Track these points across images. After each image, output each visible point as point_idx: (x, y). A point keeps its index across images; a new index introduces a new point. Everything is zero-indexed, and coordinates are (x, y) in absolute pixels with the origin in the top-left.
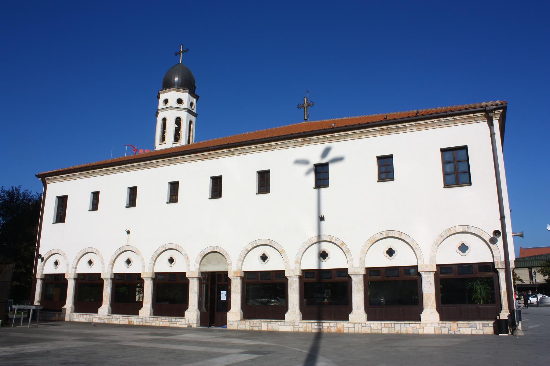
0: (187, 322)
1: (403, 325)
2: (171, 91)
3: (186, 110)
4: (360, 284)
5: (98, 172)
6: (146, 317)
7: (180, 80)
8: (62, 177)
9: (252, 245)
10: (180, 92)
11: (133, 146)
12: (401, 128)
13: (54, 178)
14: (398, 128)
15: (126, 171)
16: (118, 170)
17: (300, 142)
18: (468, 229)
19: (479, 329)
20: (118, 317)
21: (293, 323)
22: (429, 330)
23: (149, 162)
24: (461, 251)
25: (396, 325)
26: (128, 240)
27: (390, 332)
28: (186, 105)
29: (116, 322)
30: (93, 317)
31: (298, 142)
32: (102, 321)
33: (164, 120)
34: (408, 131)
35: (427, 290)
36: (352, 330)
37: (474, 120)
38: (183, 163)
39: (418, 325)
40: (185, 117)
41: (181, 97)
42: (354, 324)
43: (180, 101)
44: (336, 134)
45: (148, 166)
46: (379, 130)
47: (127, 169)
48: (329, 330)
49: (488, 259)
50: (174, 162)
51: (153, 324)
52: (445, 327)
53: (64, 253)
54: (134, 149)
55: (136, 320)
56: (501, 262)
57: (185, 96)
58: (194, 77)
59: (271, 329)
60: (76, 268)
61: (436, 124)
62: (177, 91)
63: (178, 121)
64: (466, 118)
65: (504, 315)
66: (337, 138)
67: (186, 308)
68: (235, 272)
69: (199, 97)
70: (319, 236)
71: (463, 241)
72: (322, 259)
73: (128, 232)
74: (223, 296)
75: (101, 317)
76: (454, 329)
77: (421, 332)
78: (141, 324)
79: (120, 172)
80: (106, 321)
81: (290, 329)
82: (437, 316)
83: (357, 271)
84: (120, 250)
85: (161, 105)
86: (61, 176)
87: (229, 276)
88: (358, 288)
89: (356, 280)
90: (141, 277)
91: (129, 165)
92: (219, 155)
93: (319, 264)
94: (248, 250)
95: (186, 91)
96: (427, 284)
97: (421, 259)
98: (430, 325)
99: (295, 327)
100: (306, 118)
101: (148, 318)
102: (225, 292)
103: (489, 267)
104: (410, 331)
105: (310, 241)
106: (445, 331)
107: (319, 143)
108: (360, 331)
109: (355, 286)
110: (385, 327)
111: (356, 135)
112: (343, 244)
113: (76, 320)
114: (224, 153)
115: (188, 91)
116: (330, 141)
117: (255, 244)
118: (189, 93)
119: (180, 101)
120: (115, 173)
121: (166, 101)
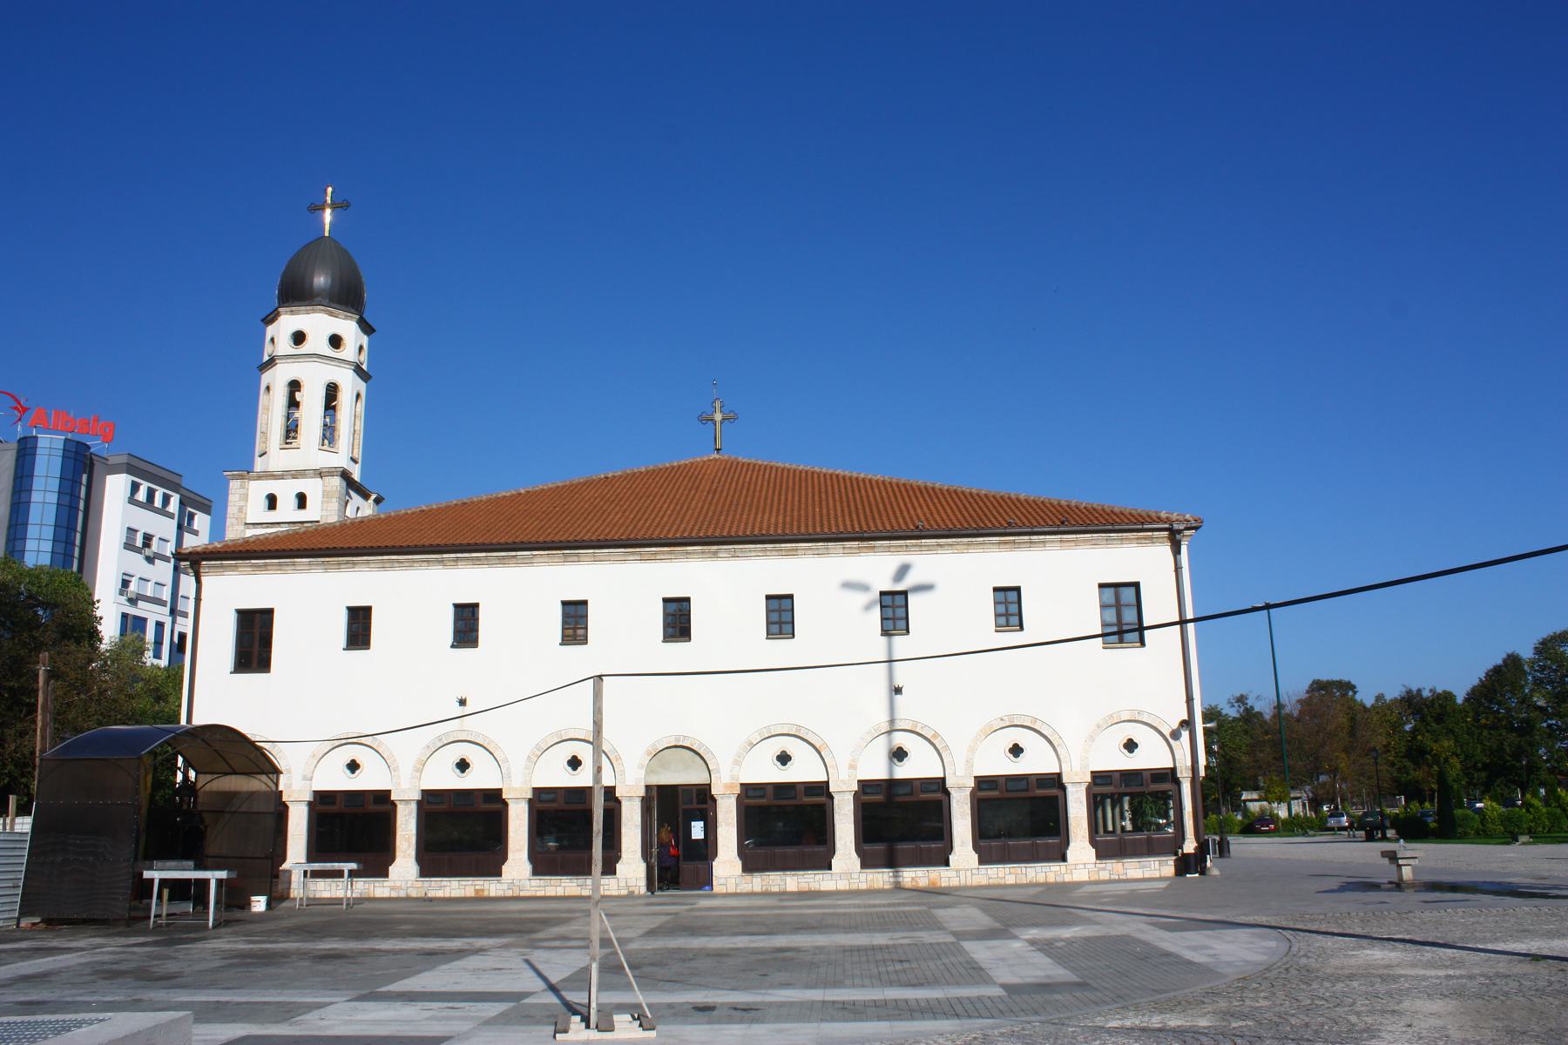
0: (622, 884)
1: (1039, 869)
2: (314, 311)
4: (966, 804)
5: (368, 562)
6: (521, 880)
7: (329, 281)
8: (253, 566)
9: (760, 734)
10: (337, 317)
11: (13, 397)
12: (1035, 543)
13: (230, 566)
14: (1031, 543)
19: (1155, 870)
20: (444, 883)
21: (848, 875)
22: (1080, 875)
23: (514, 553)
25: (1028, 869)
27: (1018, 882)
28: (349, 352)
29: (440, 894)
32: (402, 894)
36: (955, 882)
37: (1152, 540)
39: (1063, 868)
40: (349, 384)
41: (339, 332)
42: (958, 871)
43: (336, 341)
44: (923, 541)
45: (506, 561)
46: (1000, 543)
48: (914, 884)
49: (1167, 763)
50: (576, 559)
51: (539, 894)
52: (1104, 869)
54: (15, 404)
55: (492, 887)
57: (348, 328)
58: (363, 279)
59: (805, 887)
60: (311, 779)
61: (1093, 542)
62: (331, 314)
63: (332, 392)
65: (1190, 846)
66: (924, 549)
67: (504, 857)
68: (728, 786)
70: (892, 721)
72: (895, 760)
74: (697, 831)
75: (398, 884)
77: (1067, 878)
78: (509, 893)
80: (414, 894)
81: (843, 885)
82: (1091, 852)
83: (961, 782)
85: (284, 346)
86: (253, 561)
91: (459, 555)
93: (891, 771)
98: (1082, 866)
99: (851, 881)
100: (718, 446)
101: (528, 882)
102: (701, 824)
103: (1170, 775)
104: (1051, 879)
105: (875, 730)
106: (1104, 876)
108: (969, 883)
110: (1010, 873)
111: (958, 547)
112: (936, 735)
113: (326, 895)
114: (693, 553)
119: (336, 341)
121: (299, 338)
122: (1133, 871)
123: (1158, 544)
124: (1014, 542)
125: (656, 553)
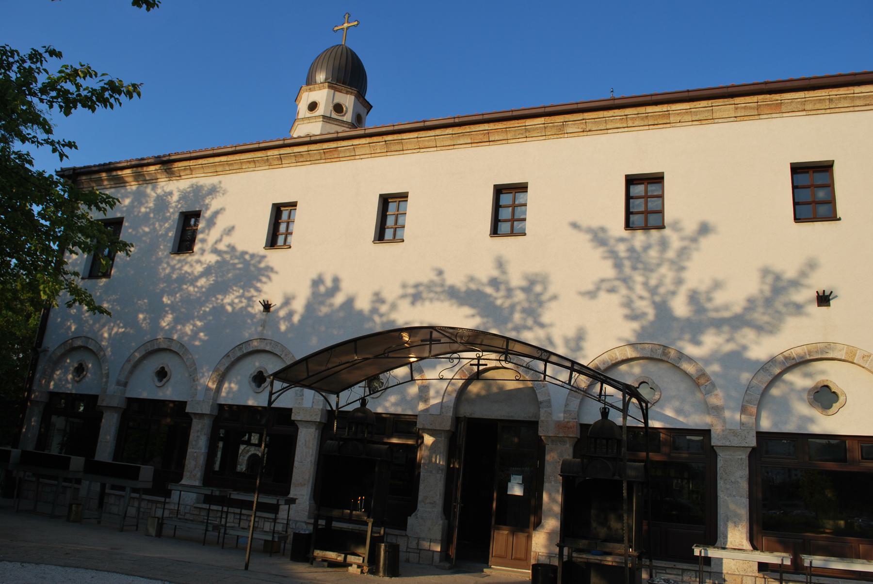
3: (349, 125)
6: (296, 522)
15: (271, 167)
16: (252, 165)
17: (751, 108)
30: (156, 508)
31: (745, 108)
38: (422, 150)
43: (338, 108)
47: (276, 162)
60: (125, 385)
66: (858, 103)
68: (560, 425)
69: (372, 107)
79: (256, 169)
84: (241, 349)
87: (541, 433)
90: (293, 418)
92: (522, 134)
95: (352, 93)
101: (304, 525)
107: (804, 113)
114: (534, 130)
115: (356, 92)
116: (837, 110)
118: (355, 96)
119: (338, 108)
120: (243, 170)
121: (313, 106)
125: (488, 133)
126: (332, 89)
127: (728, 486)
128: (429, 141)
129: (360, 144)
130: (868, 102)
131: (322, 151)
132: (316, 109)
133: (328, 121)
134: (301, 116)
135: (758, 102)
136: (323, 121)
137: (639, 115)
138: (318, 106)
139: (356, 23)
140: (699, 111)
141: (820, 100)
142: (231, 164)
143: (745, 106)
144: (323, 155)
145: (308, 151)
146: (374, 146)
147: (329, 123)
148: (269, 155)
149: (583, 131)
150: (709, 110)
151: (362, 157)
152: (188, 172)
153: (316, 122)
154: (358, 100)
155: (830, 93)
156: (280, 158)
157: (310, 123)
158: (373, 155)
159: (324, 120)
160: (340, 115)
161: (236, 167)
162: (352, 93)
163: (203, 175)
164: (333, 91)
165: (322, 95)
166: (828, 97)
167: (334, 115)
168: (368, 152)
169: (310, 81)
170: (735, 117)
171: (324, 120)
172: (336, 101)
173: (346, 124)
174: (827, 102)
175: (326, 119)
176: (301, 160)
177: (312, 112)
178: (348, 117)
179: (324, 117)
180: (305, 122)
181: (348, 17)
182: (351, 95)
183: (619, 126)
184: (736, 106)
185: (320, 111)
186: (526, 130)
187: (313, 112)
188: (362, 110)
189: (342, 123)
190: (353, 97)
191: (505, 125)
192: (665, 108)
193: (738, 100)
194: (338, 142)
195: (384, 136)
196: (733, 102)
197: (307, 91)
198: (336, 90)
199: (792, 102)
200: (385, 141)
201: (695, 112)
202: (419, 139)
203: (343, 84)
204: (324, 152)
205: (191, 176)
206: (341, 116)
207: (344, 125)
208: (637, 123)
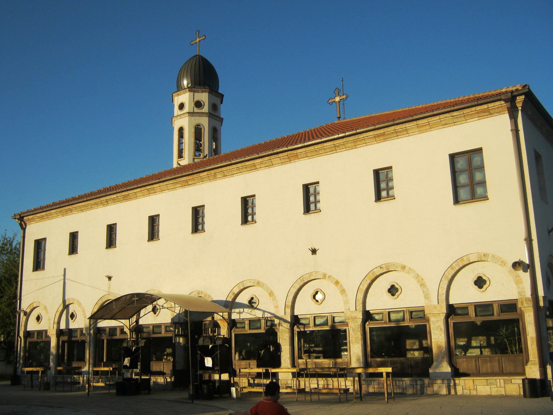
3: (207, 114)
5: (75, 208)
8: (39, 217)
9: (238, 287)
14: (396, 132)
16: (96, 206)
17: (286, 158)
18: (484, 257)
24: (484, 286)
26: (109, 288)
33: (181, 130)
34: (410, 135)
35: (437, 338)
37: (489, 113)
38: (163, 192)
46: (375, 137)
53: (45, 306)
56: (527, 299)
64: (478, 111)
71: (479, 273)
73: (110, 278)
76: (469, 387)
79: (99, 207)
84: (102, 300)
88: (356, 336)
89: (354, 327)
90: (125, 331)
94: (235, 293)
96: (436, 330)
97: (428, 298)
105: (301, 280)
109: (353, 334)
114: (205, 178)
115: (208, 90)
116: (320, 155)
117: (242, 285)
119: (198, 104)
121: (181, 106)
122: (482, 387)
123: (496, 114)
124: (384, 134)
126: (192, 92)
127: (283, 341)
128: (164, 187)
129: (137, 192)
130: (331, 150)
131: (123, 196)
132: (184, 108)
133: (192, 115)
134: (175, 114)
135: (288, 155)
136: (189, 116)
137: (243, 167)
138: (184, 106)
139: (204, 37)
140: (266, 162)
141: (312, 151)
142: (87, 206)
143: (283, 158)
144: (124, 198)
145: (117, 197)
146: (143, 192)
147: (193, 116)
148: (101, 200)
149: (224, 176)
150: (270, 161)
151: (140, 197)
152: (70, 211)
153: (185, 117)
154: (212, 94)
155: (315, 148)
156: (107, 201)
157: (181, 118)
158: (144, 196)
159: (189, 115)
160: (200, 108)
161: (90, 207)
162: (206, 91)
163: (76, 212)
164: (193, 93)
165: (184, 97)
166: (314, 150)
167: (196, 110)
168: (142, 195)
169: (179, 88)
170: (282, 163)
171: (189, 115)
172: (195, 100)
173: (205, 114)
174: (315, 151)
175: (191, 114)
176: (116, 201)
177: (181, 111)
178: (206, 109)
179: (189, 113)
180: (178, 118)
181: (198, 33)
182: (205, 92)
183: (237, 172)
184: (280, 158)
185: (186, 109)
186: (202, 178)
187: (182, 110)
188: (217, 100)
189: (202, 114)
190: (207, 94)
191: (192, 177)
192: (252, 162)
193: (280, 155)
194: (128, 191)
195: (146, 187)
196: (278, 157)
197: (176, 96)
198: (194, 92)
199: (301, 154)
200: (147, 189)
201: (264, 163)
202: (161, 187)
203: (199, 85)
204: (124, 197)
205: (72, 213)
206: (201, 109)
207: (204, 115)
208: (244, 170)
